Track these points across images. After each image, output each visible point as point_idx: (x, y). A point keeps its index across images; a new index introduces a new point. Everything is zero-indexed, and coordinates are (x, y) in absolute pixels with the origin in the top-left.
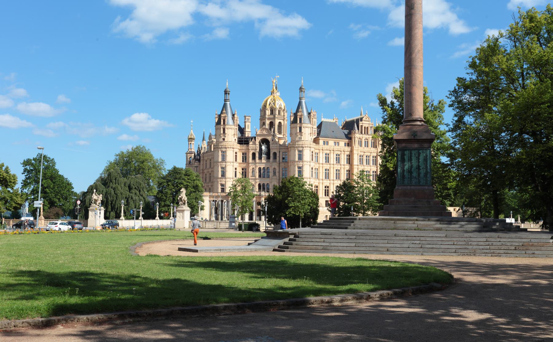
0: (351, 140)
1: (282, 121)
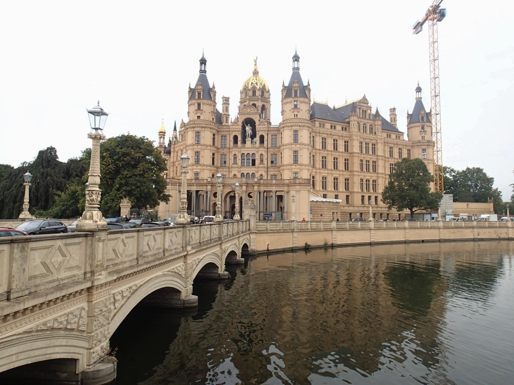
0: (349, 124)
1: (265, 104)
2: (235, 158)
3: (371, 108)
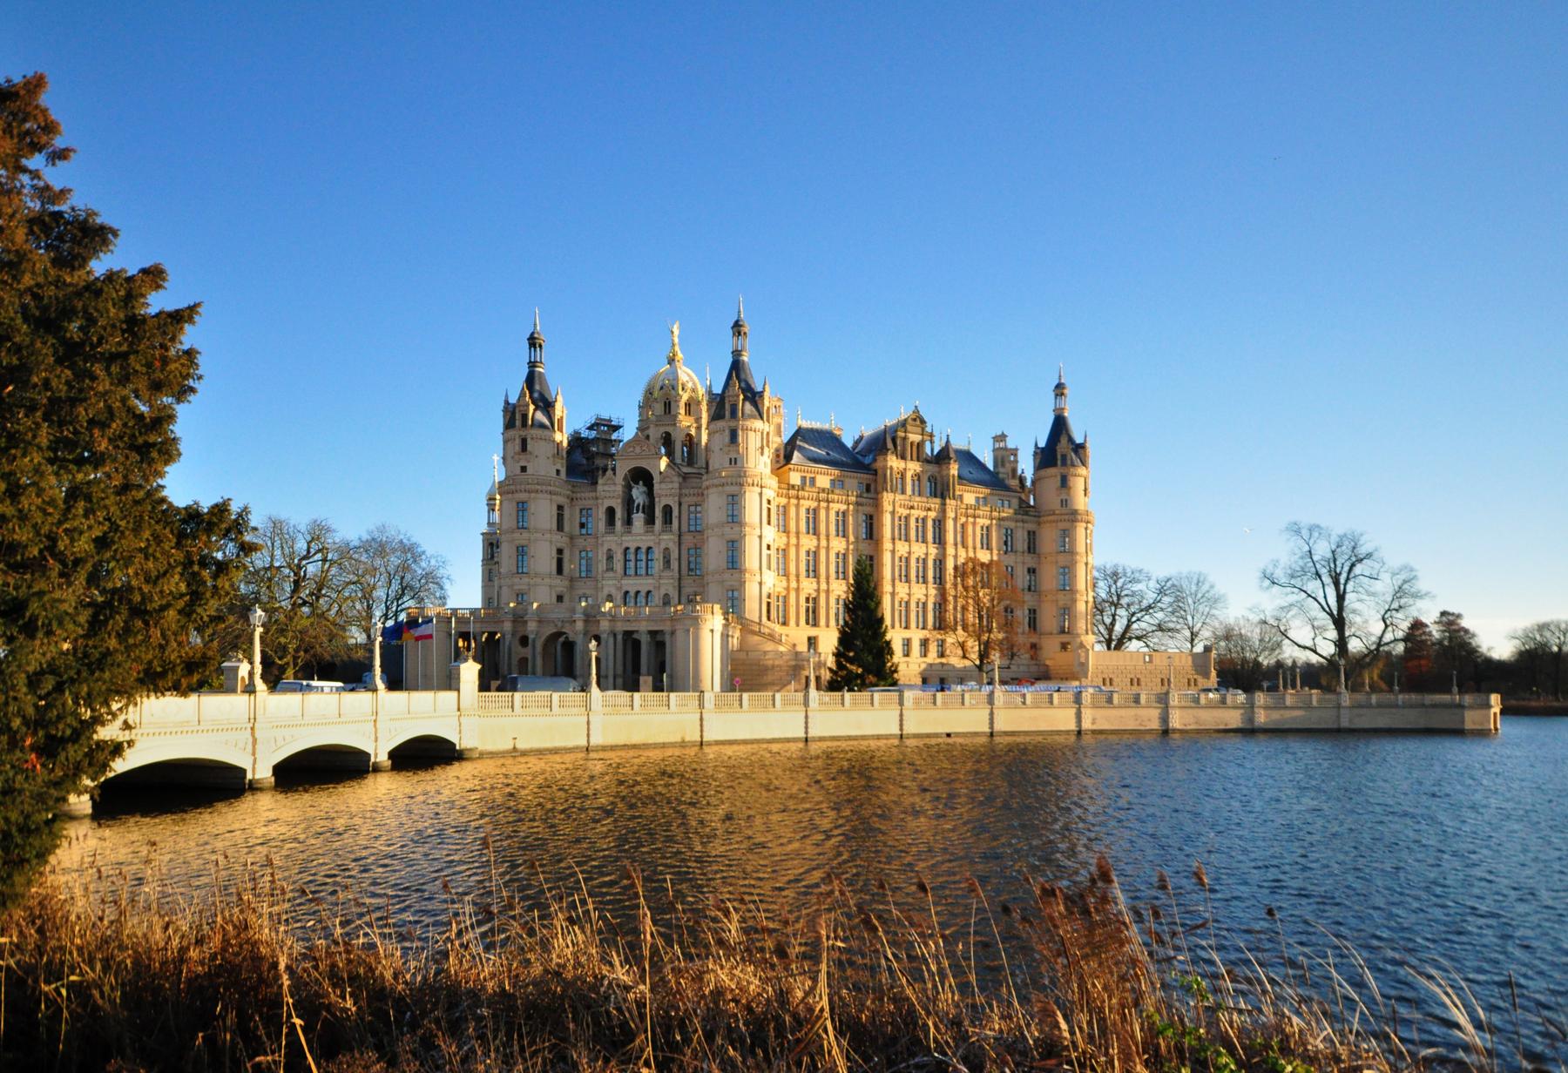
2: (610, 558)
3: (931, 435)
